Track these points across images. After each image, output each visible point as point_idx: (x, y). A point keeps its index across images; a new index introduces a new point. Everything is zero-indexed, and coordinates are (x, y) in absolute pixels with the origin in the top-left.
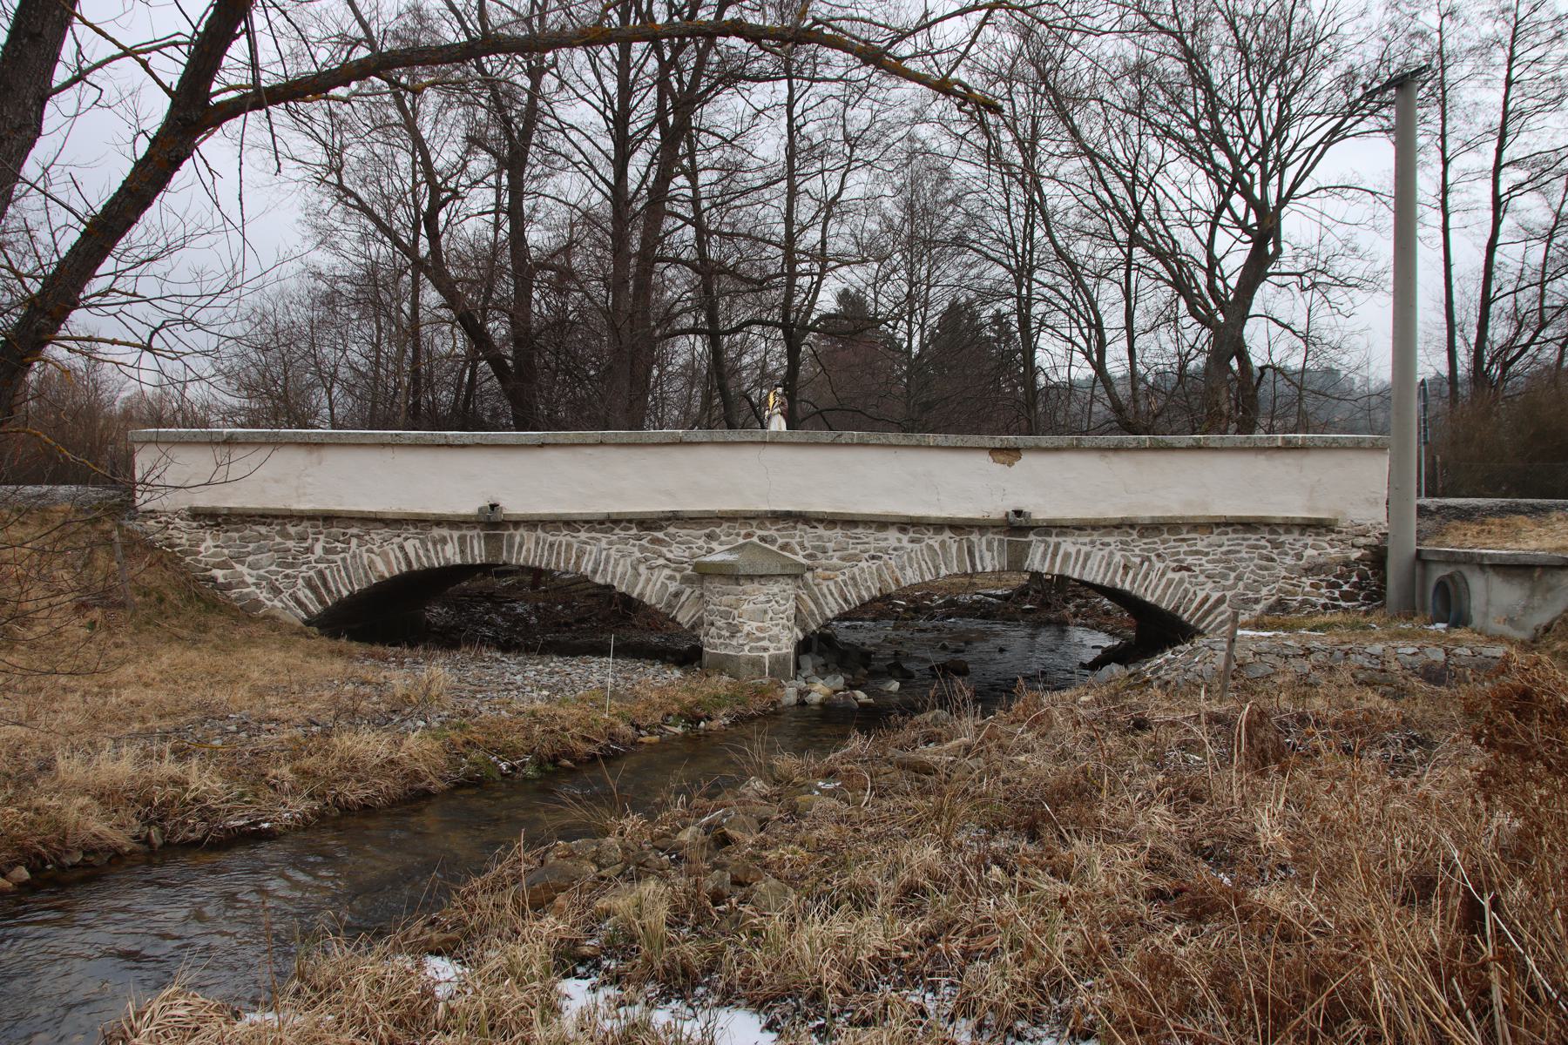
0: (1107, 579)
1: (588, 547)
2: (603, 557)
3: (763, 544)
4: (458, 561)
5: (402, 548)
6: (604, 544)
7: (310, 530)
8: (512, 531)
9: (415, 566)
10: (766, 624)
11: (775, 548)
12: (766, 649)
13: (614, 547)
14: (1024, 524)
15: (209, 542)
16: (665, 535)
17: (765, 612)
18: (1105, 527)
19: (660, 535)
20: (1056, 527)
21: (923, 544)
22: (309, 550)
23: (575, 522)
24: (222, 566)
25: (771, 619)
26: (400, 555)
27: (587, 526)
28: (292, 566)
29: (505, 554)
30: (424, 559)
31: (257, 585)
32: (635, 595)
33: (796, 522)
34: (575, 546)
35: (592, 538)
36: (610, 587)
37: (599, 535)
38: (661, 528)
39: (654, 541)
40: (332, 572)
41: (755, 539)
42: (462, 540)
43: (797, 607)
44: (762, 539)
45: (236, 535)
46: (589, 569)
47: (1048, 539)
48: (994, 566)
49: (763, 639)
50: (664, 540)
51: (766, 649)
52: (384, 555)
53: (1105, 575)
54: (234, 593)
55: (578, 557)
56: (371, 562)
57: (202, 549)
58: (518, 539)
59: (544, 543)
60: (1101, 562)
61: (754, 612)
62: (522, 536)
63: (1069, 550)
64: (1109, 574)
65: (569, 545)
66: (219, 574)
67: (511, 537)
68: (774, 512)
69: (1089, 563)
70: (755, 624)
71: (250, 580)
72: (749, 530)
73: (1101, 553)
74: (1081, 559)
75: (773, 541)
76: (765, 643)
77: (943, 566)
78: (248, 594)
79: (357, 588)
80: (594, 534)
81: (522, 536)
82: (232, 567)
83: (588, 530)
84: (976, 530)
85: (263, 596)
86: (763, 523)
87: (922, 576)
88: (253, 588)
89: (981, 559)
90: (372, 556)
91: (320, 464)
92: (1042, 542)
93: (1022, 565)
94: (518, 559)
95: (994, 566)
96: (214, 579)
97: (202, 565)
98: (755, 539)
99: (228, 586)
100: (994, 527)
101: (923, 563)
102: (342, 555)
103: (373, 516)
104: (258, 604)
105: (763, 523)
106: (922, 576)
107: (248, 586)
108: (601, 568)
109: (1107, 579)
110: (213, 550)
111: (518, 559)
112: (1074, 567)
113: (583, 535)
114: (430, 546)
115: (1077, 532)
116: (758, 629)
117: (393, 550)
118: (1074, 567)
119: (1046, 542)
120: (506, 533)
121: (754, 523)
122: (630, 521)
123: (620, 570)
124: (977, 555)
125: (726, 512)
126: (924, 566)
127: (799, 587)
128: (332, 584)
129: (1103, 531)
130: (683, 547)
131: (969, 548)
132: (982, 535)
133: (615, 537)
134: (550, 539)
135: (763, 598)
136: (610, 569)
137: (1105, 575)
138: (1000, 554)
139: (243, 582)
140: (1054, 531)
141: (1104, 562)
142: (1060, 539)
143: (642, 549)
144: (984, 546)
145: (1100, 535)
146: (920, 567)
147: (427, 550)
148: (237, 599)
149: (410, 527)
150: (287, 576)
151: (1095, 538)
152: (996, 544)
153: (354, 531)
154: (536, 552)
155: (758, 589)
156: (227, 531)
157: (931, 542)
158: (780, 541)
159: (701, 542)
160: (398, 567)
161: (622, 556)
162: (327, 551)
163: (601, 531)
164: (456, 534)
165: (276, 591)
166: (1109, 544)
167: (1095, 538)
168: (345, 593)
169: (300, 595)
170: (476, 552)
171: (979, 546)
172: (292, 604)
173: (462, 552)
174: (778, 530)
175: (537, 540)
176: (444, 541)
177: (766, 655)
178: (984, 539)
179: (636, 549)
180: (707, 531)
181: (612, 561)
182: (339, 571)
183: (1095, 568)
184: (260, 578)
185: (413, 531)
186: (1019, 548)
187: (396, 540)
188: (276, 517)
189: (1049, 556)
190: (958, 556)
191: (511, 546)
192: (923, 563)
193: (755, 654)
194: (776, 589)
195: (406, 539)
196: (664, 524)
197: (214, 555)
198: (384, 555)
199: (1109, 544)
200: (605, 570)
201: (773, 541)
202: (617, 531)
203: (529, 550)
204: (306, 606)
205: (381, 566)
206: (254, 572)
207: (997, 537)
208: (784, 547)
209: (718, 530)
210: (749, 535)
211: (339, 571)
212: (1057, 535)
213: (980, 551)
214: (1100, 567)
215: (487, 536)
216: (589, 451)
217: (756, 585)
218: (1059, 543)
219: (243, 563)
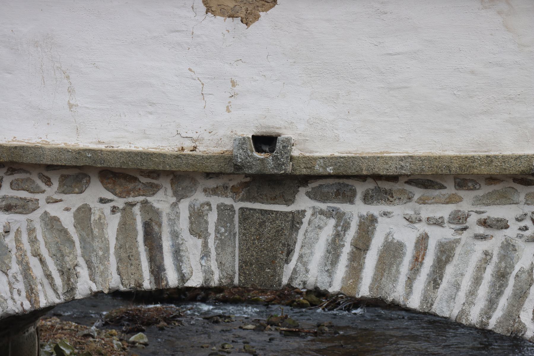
0: (497, 315)
14: (270, 167)
18: (491, 179)
20: (363, 178)
21: (36, 216)
47: (344, 207)
48: (208, 272)
53: (492, 303)
60: (481, 269)
63: (398, 237)
64: (503, 302)
69: (449, 270)
73: (481, 246)
74: (429, 261)
77: (83, 272)
84: (165, 183)
87: (31, 293)
89: (177, 253)
92: (328, 214)
93: (276, 274)
95: (208, 272)
100: (208, 175)
101: (34, 262)
106: (31, 293)
109: (497, 315)
112: (410, 281)
115: (418, 193)
118: (410, 281)
119: (339, 216)
124: (167, 245)
126: (37, 271)
129: (485, 190)
131: (147, 226)
132: (180, 196)
137: (492, 303)
138: (221, 245)
140: (360, 189)
141: (490, 270)
142: (375, 209)
144: (184, 224)
145: (478, 201)
146: (26, 271)
151: (465, 206)
152: (212, 218)
157: (54, 210)
166: (502, 225)
167: (465, 206)
171: (173, 222)
178: (184, 206)
183: (466, 284)
186: (268, 230)
189: (347, 249)
190: (120, 247)
192: (34, 262)
199: (502, 225)
207: (215, 201)
212: (367, 199)
213: (175, 235)
214: (477, 281)
218: (373, 220)
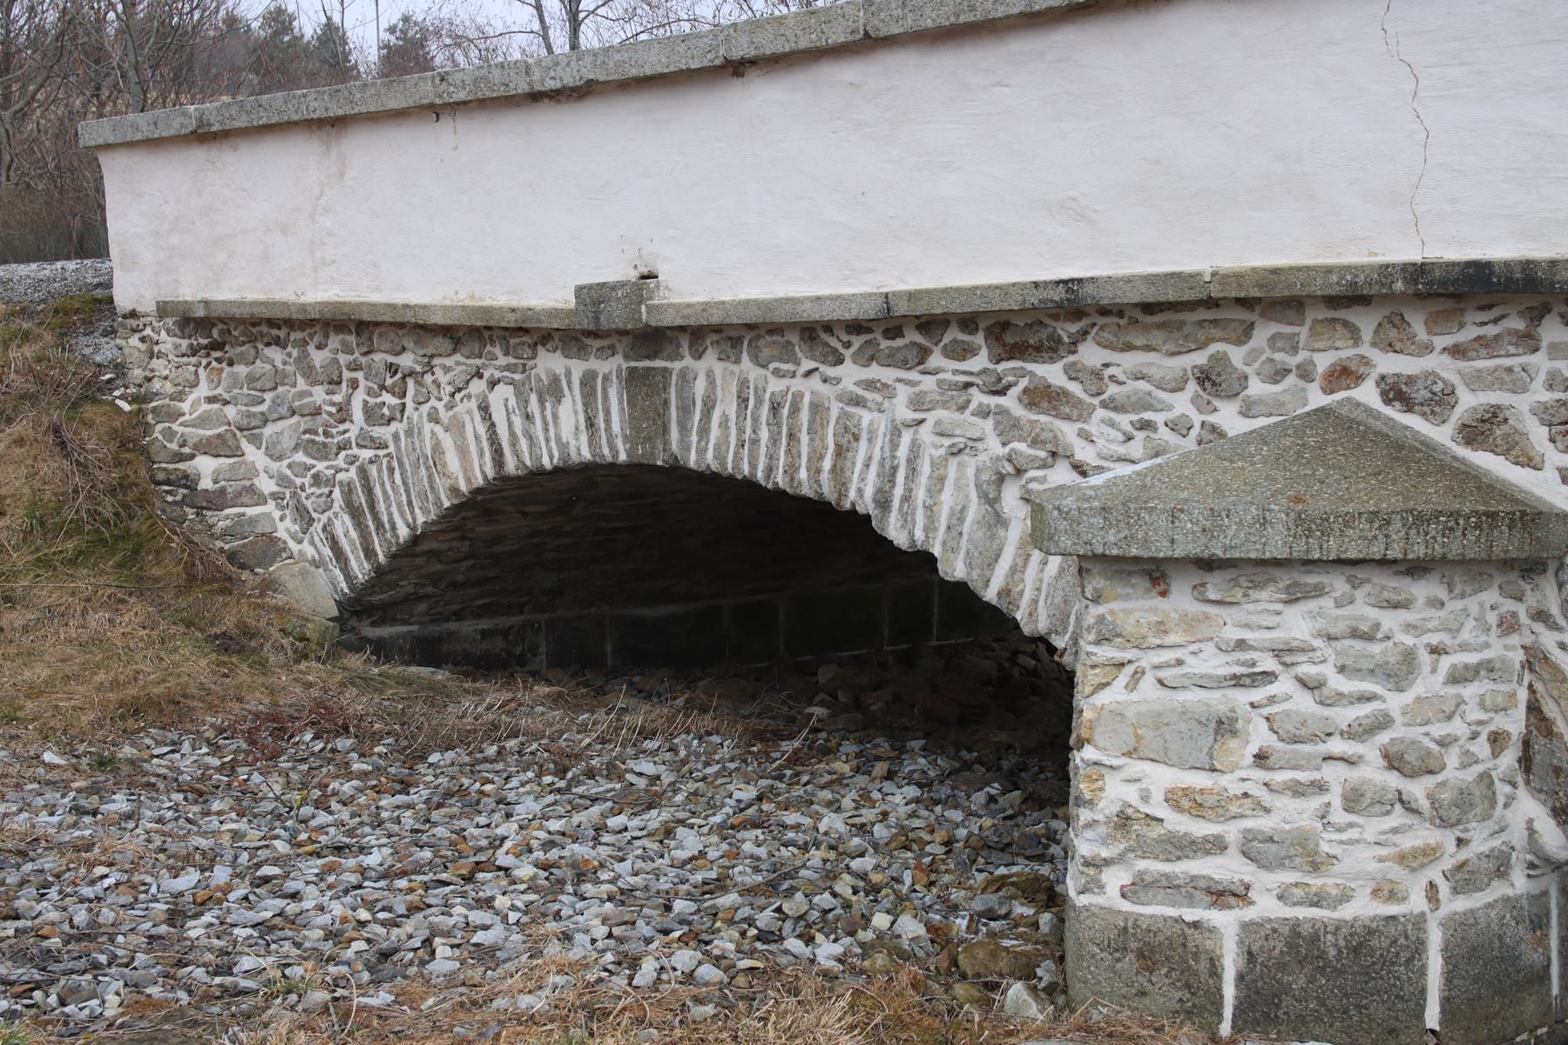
1: (866, 417)
2: (902, 452)
3: (1394, 413)
4: (587, 455)
5: (484, 409)
6: (905, 413)
7: (343, 359)
8: (688, 361)
9: (511, 466)
10: (1229, 783)
11: (1442, 434)
12: (1221, 895)
13: (932, 417)
15: (203, 390)
16: (1073, 373)
17: (1225, 727)
19: (1052, 373)
22: (343, 413)
23: (828, 327)
24: (219, 447)
25: (1261, 758)
26: (482, 430)
27: (858, 341)
28: (322, 452)
29: (674, 434)
30: (523, 444)
31: (277, 497)
32: (990, 595)
33: (1537, 315)
34: (835, 409)
35: (870, 385)
36: (925, 560)
37: (888, 375)
38: (1051, 349)
39: (1042, 397)
40: (380, 471)
41: (1367, 394)
42: (588, 381)
43: (1534, 708)
44: (1395, 392)
45: (241, 370)
46: (869, 492)
49: (1215, 846)
50: (1063, 394)
51: (1221, 895)
52: (456, 428)
54: (221, 520)
55: (840, 452)
56: (437, 448)
57: (185, 406)
58: (700, 387)
59: (759, 402)
61: (1157, 720)
62: (710, 375)
65: (818, 408)
66: (206, 468)
67: (686, 379)
68: (1417, 271)
70: (1162, 778)
71: (266, 485)
72: (1347, 353)
75: (1439, 402)
76: (1226, 868)
78: (253, 521)
79: (421, 519)
80: (875, 372)
81: (710, 375)
82: (237, 452)
83: (869, 357)
85: (285, 528)
86: (1397, 321)
88: (270, 507)
90: (438, 429)
91: (342, 174)
94: (702, 452)
96: (189, 481)
97: (174, 446)
98: (1367, 394)
99: (217, 500)
102: (394, 426)
103: (409, 317)
104: (271, 547)
105: (1397, 321)
107: (261, 500)
108: (898, 491)
110: (205, 407)
111: (702, 452)
113: (850, 374)
114: (533, 399)
116: (1185, 801)
117: (469, 412)
120: (676, 366)
121: (1366, 321)
122: (968, 322)
123: (947, 498)
125: (1237, 277)
127: (1541, 616)
128: (381, 506)
130: (1124, 420)
133: (929, 383)
134: (776, 385)
135: (1212, 663)
136: (920, 495)
139: (252, 490)
143: (1008, 428)
147: (528, 417)
148: (224, 534)
149: (498, 351)
150: (317, 480)
153: (406, 361)
154: (741, 430)
155: (1189, 623)
156: (231, 364)
158: (1468, 401)
159: (1182, 404)
160: (481, 471)
161: (956, 452)
162: (371, 414)
163: (891, 360)
164: (578, 367)
165: (304, 517)
168: (403, 532)
169: (339, 531)
170: (616, 427)
172: (327, 552)
173: (590, 424)
174: (1457, 351)
175: (743, 383)
176: (553, 390)
177: (1225, 921)
179: (988, 425)
180: (1200, 358)
181: (925, 469)
182: (391, 470)
184: (283, 481)
185: (503, 360)
187: (477, 386)
188: (290, 324)
191: (685, 409)
193: (1156, 910)
194: (1297, 623)
195: (493, 384)
196: (1065, 330)
197: (203, 421)
198: (456, 428)
200: (907, 498)
201: (1439, 402)
202: (936, 360)
203: (724, 424)
204: (346, 561)
205: (453, 463)
206: (274, 466)
208: (1479, 431)
209: (1236, 355)
210: (1344, 375)
211: (391, 470)
215: (635, 381)
216: (847, 72)
217: (1181, 600)
219: (256, 440)
